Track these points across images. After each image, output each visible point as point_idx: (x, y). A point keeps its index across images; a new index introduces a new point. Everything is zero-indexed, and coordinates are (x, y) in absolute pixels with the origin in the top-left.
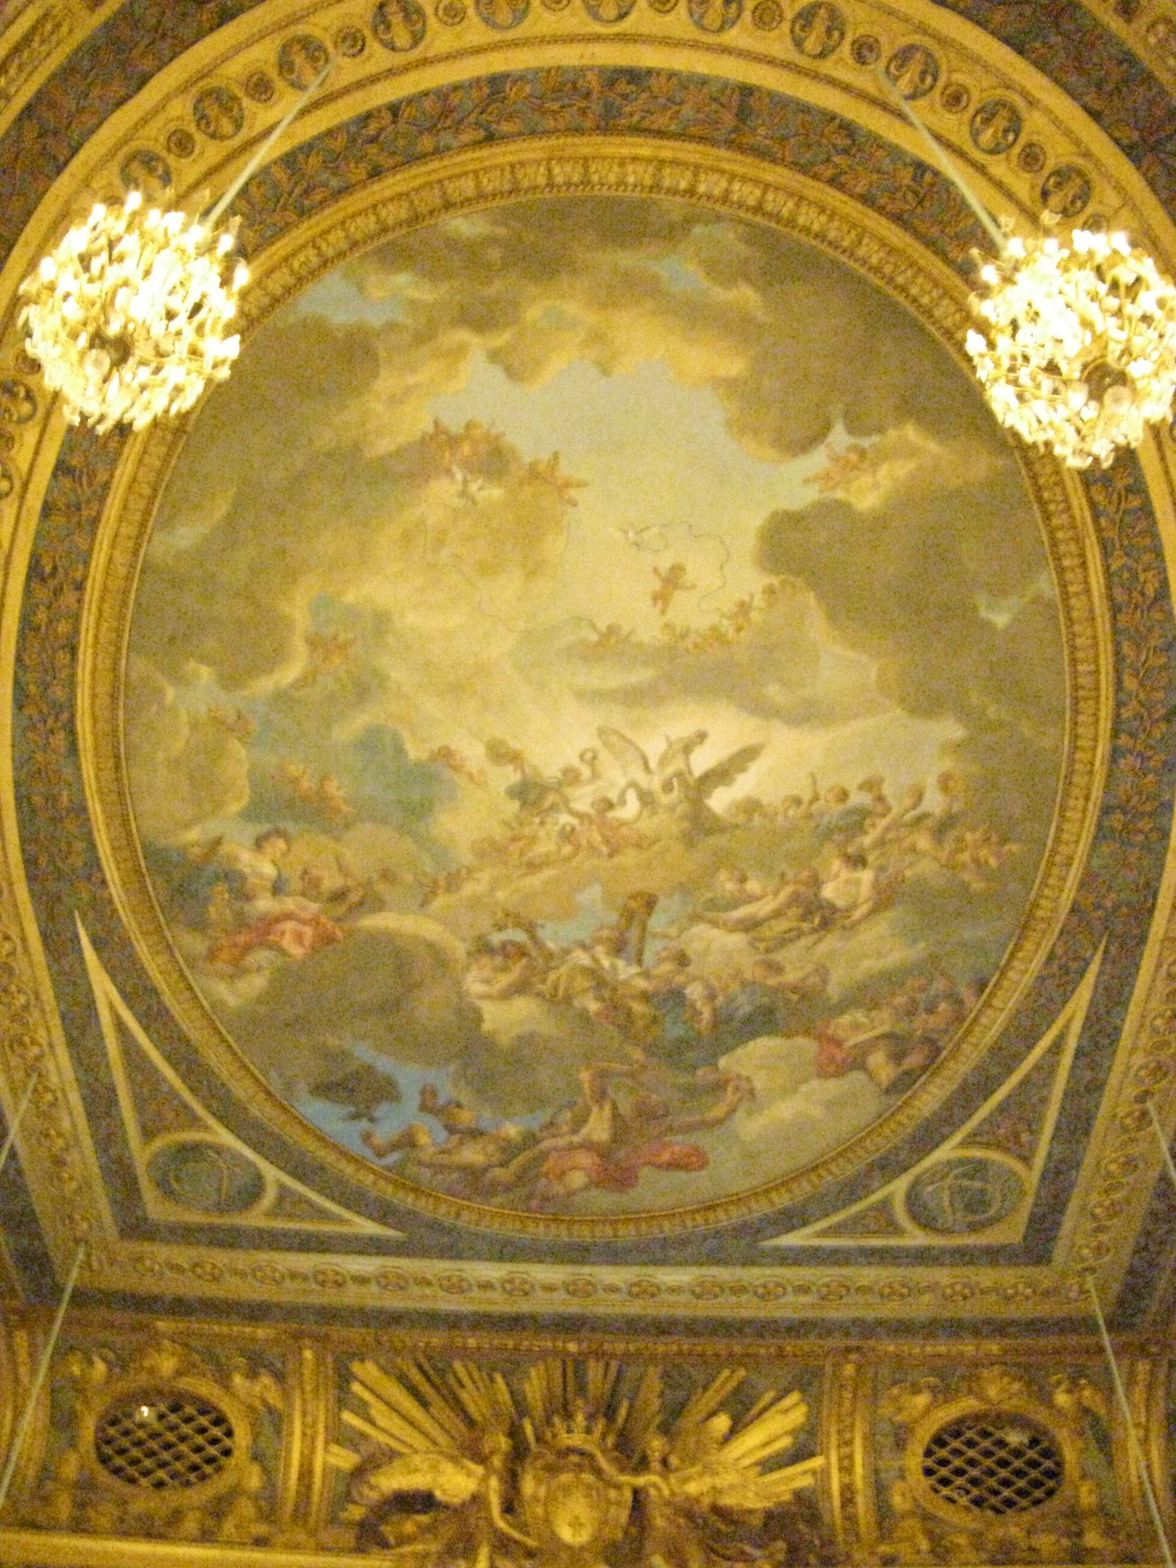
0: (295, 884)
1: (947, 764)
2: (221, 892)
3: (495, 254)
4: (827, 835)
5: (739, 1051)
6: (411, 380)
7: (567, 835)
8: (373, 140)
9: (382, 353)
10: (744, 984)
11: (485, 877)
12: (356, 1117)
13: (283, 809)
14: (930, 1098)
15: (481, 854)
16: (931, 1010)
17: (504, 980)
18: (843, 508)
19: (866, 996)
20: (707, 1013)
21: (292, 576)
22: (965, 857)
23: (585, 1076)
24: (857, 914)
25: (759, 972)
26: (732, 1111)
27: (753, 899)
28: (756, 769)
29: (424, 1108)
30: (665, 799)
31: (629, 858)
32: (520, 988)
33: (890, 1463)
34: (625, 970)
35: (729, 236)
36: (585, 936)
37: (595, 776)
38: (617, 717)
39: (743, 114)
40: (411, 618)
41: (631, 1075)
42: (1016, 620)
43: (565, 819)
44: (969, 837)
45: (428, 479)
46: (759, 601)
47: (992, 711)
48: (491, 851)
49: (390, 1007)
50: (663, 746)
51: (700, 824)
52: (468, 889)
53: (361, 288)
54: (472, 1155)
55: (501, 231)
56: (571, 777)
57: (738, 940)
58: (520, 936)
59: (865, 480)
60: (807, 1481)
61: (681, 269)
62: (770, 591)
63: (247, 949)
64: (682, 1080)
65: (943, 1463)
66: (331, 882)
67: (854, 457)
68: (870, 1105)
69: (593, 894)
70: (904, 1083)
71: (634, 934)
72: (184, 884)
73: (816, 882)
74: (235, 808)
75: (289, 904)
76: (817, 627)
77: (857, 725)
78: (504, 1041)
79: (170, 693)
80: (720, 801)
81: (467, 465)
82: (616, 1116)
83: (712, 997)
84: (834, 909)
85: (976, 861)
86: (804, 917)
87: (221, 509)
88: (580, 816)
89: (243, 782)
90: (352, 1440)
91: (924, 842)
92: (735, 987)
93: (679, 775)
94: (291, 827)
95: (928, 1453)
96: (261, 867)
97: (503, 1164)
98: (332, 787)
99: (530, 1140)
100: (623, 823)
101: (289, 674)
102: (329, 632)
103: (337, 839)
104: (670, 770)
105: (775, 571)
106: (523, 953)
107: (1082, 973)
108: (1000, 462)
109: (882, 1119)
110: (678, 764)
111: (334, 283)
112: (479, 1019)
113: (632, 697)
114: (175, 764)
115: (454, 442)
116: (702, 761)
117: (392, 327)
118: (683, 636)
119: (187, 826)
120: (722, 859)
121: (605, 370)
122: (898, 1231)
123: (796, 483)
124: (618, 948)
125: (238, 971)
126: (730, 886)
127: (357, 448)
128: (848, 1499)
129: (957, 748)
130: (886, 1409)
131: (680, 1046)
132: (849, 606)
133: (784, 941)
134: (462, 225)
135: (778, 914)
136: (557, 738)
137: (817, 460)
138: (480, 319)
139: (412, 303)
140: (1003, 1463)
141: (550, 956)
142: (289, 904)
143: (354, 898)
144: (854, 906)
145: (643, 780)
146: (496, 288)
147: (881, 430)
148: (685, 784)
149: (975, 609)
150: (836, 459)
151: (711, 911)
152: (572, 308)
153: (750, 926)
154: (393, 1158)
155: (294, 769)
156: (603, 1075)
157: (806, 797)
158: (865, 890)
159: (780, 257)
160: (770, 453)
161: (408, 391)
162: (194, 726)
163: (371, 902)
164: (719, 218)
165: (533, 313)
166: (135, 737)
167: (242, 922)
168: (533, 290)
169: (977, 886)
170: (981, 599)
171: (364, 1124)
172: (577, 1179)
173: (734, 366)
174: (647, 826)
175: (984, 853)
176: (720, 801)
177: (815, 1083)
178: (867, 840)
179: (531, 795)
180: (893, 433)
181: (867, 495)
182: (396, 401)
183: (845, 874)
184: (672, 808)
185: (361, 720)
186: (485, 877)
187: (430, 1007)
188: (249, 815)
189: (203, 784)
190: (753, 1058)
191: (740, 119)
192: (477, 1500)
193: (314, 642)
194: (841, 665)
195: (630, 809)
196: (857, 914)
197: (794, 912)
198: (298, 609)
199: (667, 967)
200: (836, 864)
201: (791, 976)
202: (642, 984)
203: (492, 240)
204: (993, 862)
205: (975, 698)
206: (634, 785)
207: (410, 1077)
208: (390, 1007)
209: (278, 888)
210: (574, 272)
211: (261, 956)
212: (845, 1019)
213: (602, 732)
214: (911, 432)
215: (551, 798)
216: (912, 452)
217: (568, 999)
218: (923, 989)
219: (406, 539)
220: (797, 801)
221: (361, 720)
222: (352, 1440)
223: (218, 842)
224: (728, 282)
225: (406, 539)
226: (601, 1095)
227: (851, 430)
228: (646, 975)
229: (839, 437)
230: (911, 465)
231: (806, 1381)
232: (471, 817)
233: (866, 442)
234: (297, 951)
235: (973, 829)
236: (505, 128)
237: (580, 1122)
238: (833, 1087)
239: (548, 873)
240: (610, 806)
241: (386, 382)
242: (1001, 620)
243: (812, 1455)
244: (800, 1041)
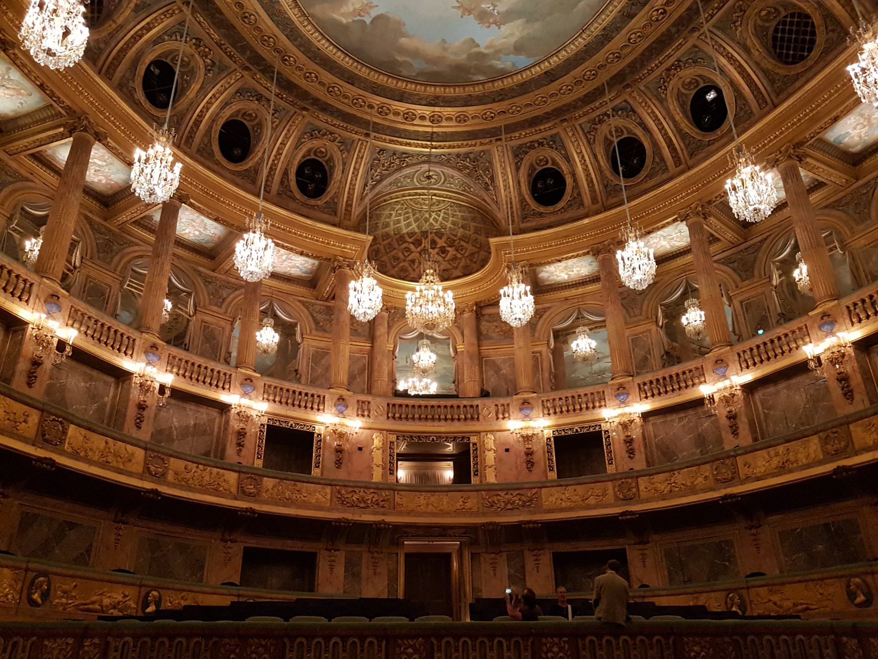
3: (472, 71)
6: (504, 40)
9: (512, 48)
35: (405, 72)
39: (402, 96)
45: (507, 11)
61: (418, 65)
81: (492, 14)
108: (311, 11)
111: (521, 66)
115: (495, 23)
121: (444, 41)
127: (527, 22)
138: (482, 56)
139: (499, 60)
147: (354, 21)
150: (368, 13)
152: (452, 57)
159: (391, 68)
160: (390, 16)
165: (464, 56)
173: (403, 40)
182: (512, 35)
191: (402, 97)
203: (474, 74)
214: (344, 21)
216: (343, 15)
224: (405, 61)
229: (368, 20)
233: (358, 18)
241: (512, 40)
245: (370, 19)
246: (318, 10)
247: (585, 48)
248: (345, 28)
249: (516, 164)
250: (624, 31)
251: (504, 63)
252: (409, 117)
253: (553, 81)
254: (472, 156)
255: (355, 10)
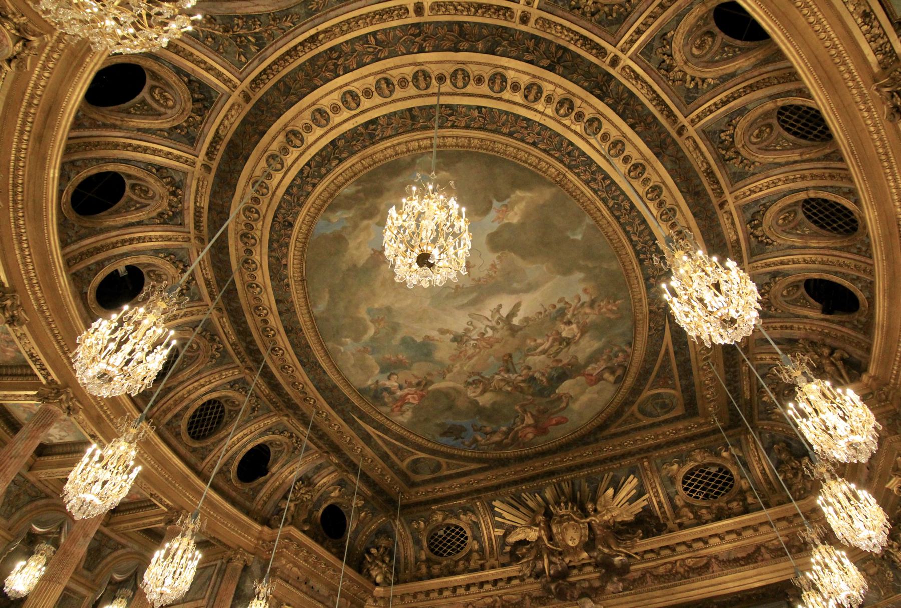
0: (405, 385)
1: (583, 286)
2: (385, 394)
3: (362, 195)
4: (555, 319)
5: (560, 387)
6: (359, 240)
7: (475, 346)
8: (308, 176)
10: (552, 368)
11: (458, 365)
12: (457, 439)
13: (389, 368)
14: (629, 381)
15: (453, 360)
16: (617, 356)
17: (479, 391)
18: (509, 225)
19: (593, 358)
20: (544, 380)
21: (357, 307)
22: (604, 310)
23: (517, 408)
24: (577, 338)
25: (555, 364)
26: (567, 405)
27: (541, 345)
28: (522, 308)
29: (474, 431)
30: (498, 327)
31: (497, 346)
32: (484, 392)
33: (671, 490)
34: (513, 376)
36: (496, 371)
37: (474, 328)
38: (472, 310)
39: (413, 118)
40: (397, 305)
41: (531, 403)
42: (584, 235)
43: (472, 342)
44: (602, 304)
45: (379, 266)
46: (497, 262)
47: (590, 265)
48: (455, 358)
49: (450, 408)
50: (490, 313)
51: (513, 330)
52: (455, 370)
53: (329, 221)
54: (496, 438)
55: (360, 187)
56: (467, 330)
57: (543, 357)
58: (476, 378)
59: (511, 214)
60: (646, 503)
62: (499, 257)
63: (401, 406)
64: (547, 400)
65: (690, 485)
66: (415, 381)
67: (504, 208)
68: (612, 389)
69: (492, 359)
70: (619, 380)
71: (510, 366)
72: (377, 395)
73: (558, 333)
74: (377, 371)
75: (406, 391)
76: (520, 262)
77: (549, 284)
78: (488, 406)
79: (342, 349)
80: (515, 321)
82: (532, 416)
83: (543, 375)
84: (569, 339)
85: (608, 310)
86: (560, 344)
87: (327, 296)
88: (476, 340)
89: (375, 364)
90: (500, 526)
91: (588, 310)
92: (549, 370)
93: (499, 319)
94: (396, 371)
95: (684, 483)
96: (393, 384)
97: (506, 438)
98: (401, 357)
99: (510, 430)
100: (490, 338)
101: (372, 332)
102: (376, 317)
103: (410, 370)
104: (496, 318)
105: (497, 252)
106: (481, 382)
107: (664, 329)
108: (554, 190)
109: (618, 391)
110: (497, 316)
112: (477, 403)
113: (474, 302)
114: (354, 366)
116: (504, 312)
117: (344, 228)
118: (479, 280)
119: (367, 380)
120: (525, 337)
122: (639, 420)
123: (491, 222)
124: (508, 371)
125: (403, 413)
126: (532, 344)
127: (355, 266)
128: (661, 506)
129: (584, 280)
130: (664, 473)
131: (544, 390)
132: (526, 253)
133: (557, 353)
134: (347, 190)
135: (551, 346)
136: (458, 322)
137: (493, 214)
140: (712, 480)
141: (488, 380)
142: (406, 391)
143: (424, 383)
144: (575, 336)
145: (489, 324)
146: (368, 205)
147: (508, 196)
148: (502, 321)
149: (568, 237)
150: (498, 211)
151: (530, 351)
153: (544, 352)
154: (473, 446)
155: (387, 356)
156: (522, 406)
157: (543, 311)
158: (576, 330)
159: (449, 158)
161: (360, 244)
162: (353, 355)
163: (429, 383)
164: (423, 154)
166: (340, 363)
167: (396, 400)
168: (379, 200)
169: (612, 316)
170: (569, 234)
171: (460, 440)
172: (530, 436)
174: (497, 335)
175: (610, 307)
176: (515, 321)
177: (590, 388)
178: (569, 316)
179: (457, 339)
180: (512, 196)
181: (514, 217)
182: (358, 248)
183: (567, 328)
184: (502, 328)
185: (399, 337)
186: (458, 365)
187: (461, 404)
188: (382, 372)
189: (365, 368)
190: (566, 387)
191: (412, 119)
192: (539, 538)
193: (372, 321)
194: (533, 270)
195: (490, 333)
196: (577, 338)
197: (557, 343)
198: (363, 313)
199: (524, 372)
200: (562, 326)
201: (565, 361)
202: (520, 378)
203: (358, 192)
204: (614, 308)
205: (582, 263)
206: (487, 326)
207: (464, 422)
208: (450, 408)
209: (401, 388)
210: (388, 190)
211: (405, 407)
212: (589, 368)
213: (469, 315)
215: (465, 338)
216: (522, 198)
217: (500, 389)
218: (611, 352)
219: (383, 284)
220: (540, 313)
221: (399, 337)
222: (500, 526)
223: (377, 382)
225: (383, 284)
226: (525, 411)
227: (498, 200)
228: (520, 376)
229: (496, 204)
230: (523, 203)
231: (633, 471)
232: (445, 351)
233: (505, 202)
234: (416, 402)
235: (602, 301)
236: (344, 155)
237: (523, 421)
238: (596, 388)
239: (475, 359)
240: (484, 334)
241: (352, 244)
242: (579, 237)
243: (645, 494)
244: (578, 378)
245: (493, 206)
246: (546, 194)
247: (284, 261)
248: (516, 184)
249: (188, 75)
250: (270, 290)
251: (339, 218)
252: (386, 85)
253: (275, 216)
254: (253, 48)
255: (512, 209)
